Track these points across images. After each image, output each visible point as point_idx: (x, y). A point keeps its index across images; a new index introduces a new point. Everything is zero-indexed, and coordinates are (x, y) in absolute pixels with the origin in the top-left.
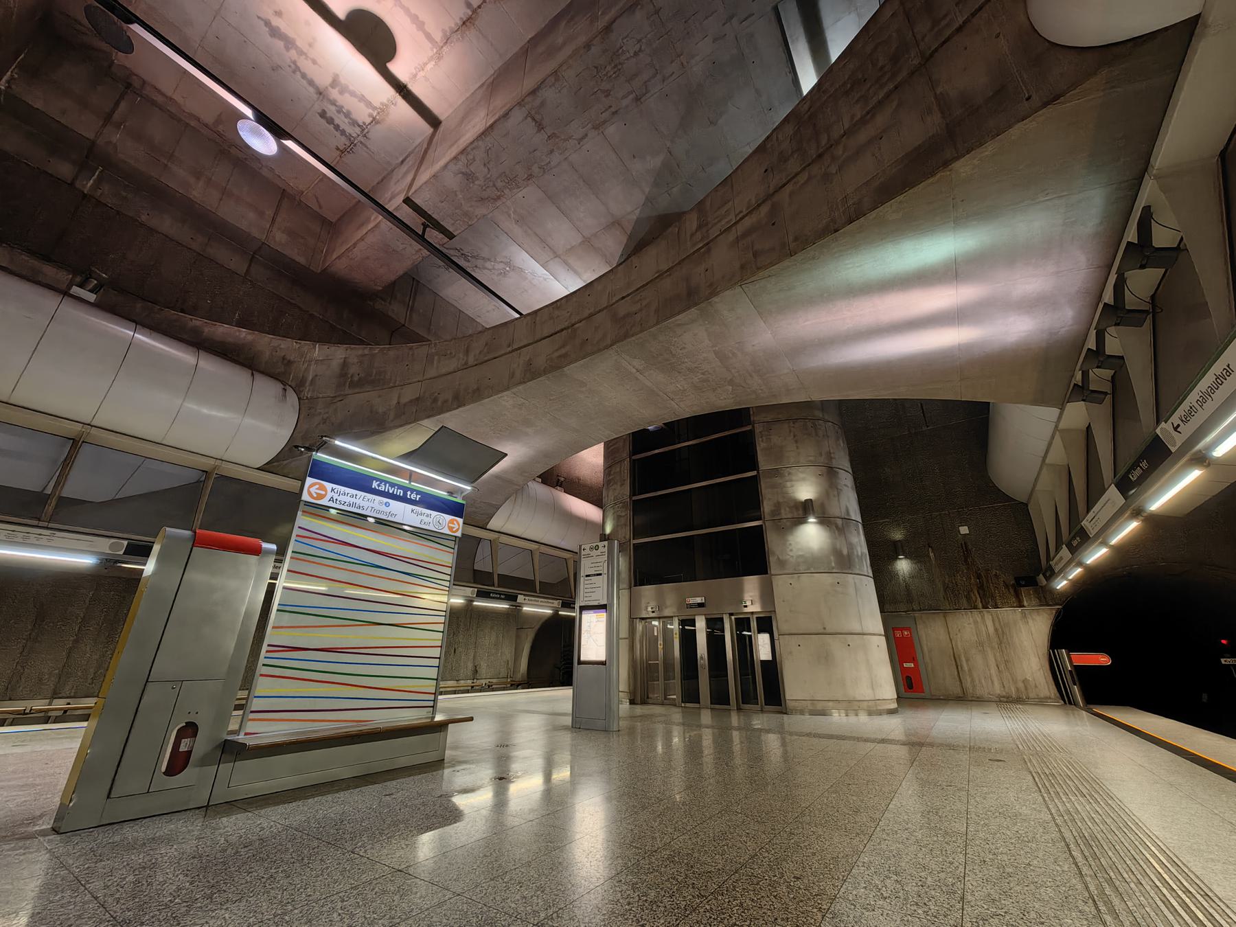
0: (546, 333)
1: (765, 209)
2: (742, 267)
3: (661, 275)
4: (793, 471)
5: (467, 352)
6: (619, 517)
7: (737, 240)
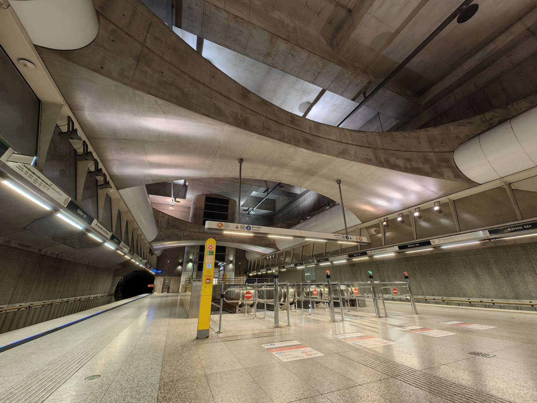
5: (200, 229)
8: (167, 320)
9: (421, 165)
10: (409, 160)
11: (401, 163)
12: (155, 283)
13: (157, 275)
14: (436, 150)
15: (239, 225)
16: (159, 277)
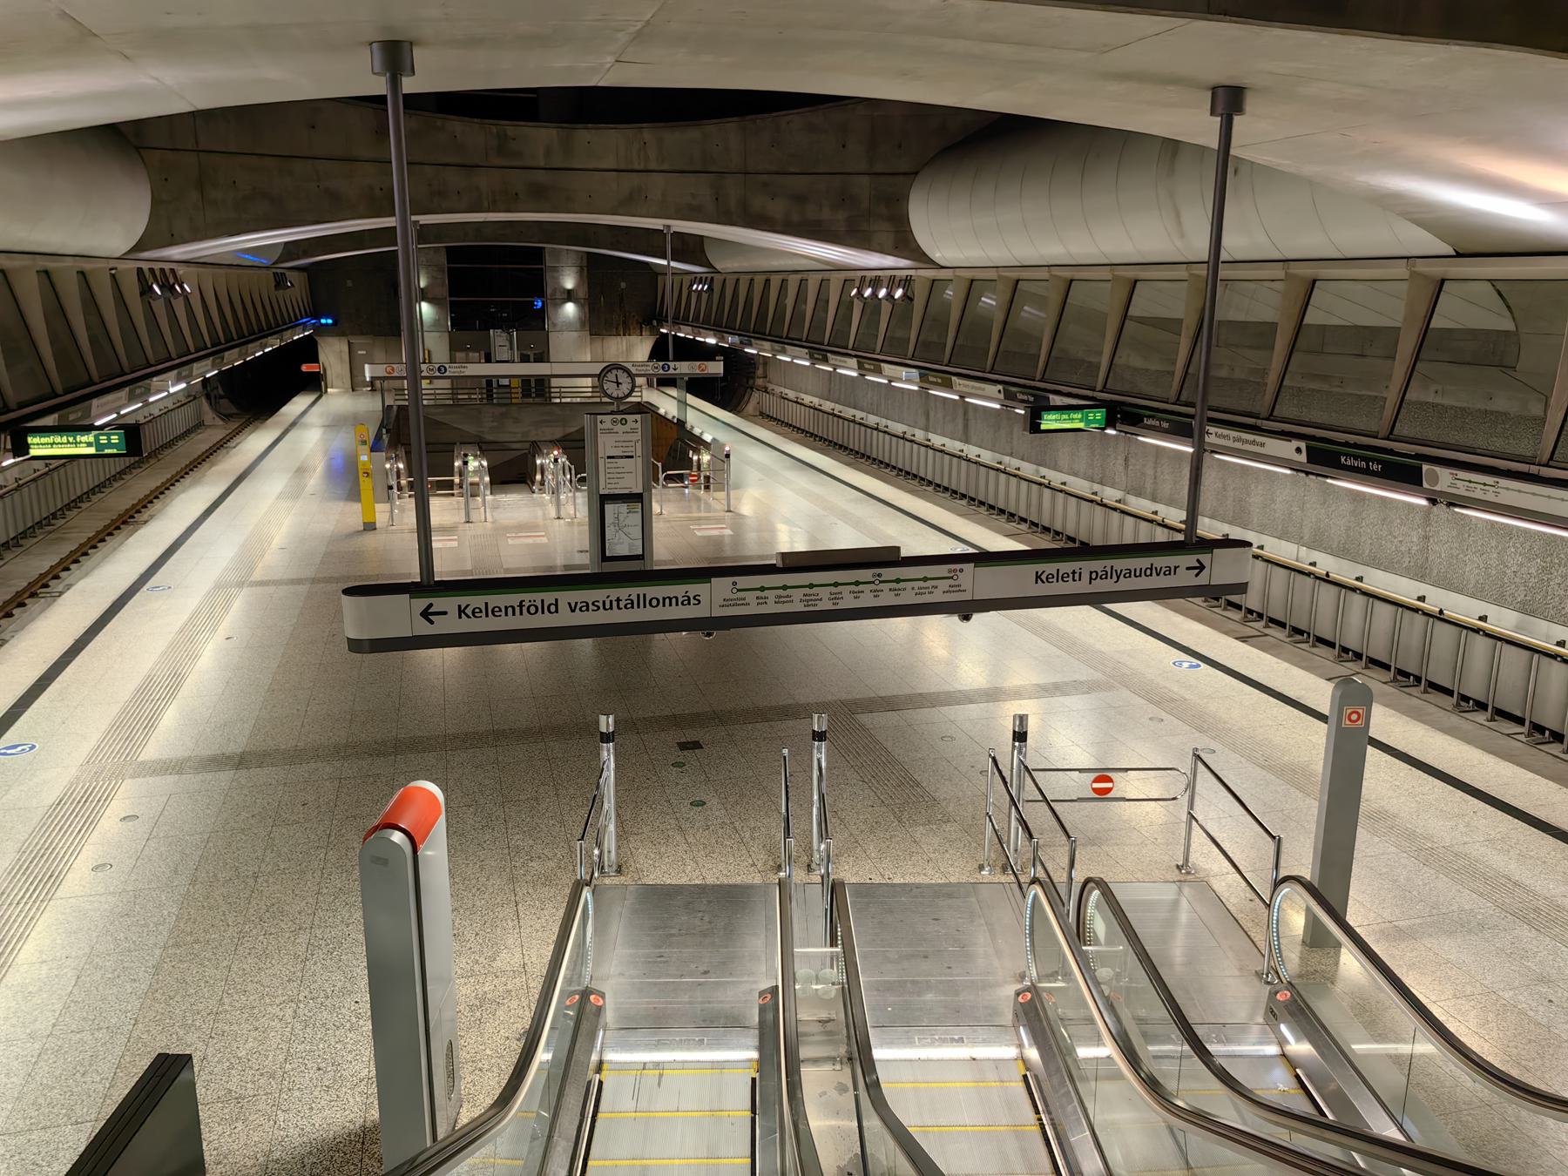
8: (342, 504)
9: (826, 214)
10: (800, 199)
11: (777, 208)
12: (322, 357)
13: (321, 330)
14: (879, 168)
16: (330, 340)
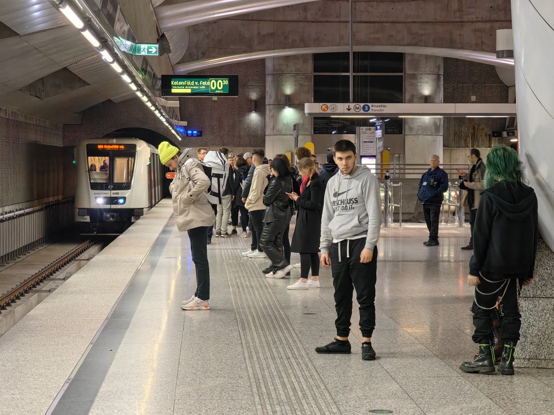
0: (364, 19)
1: (488, 25)
2: (476, 45)
3: (437, 22)
4: (423, 76)
6: (301, 85)
7: (475, 30)
15: (352, 105)
